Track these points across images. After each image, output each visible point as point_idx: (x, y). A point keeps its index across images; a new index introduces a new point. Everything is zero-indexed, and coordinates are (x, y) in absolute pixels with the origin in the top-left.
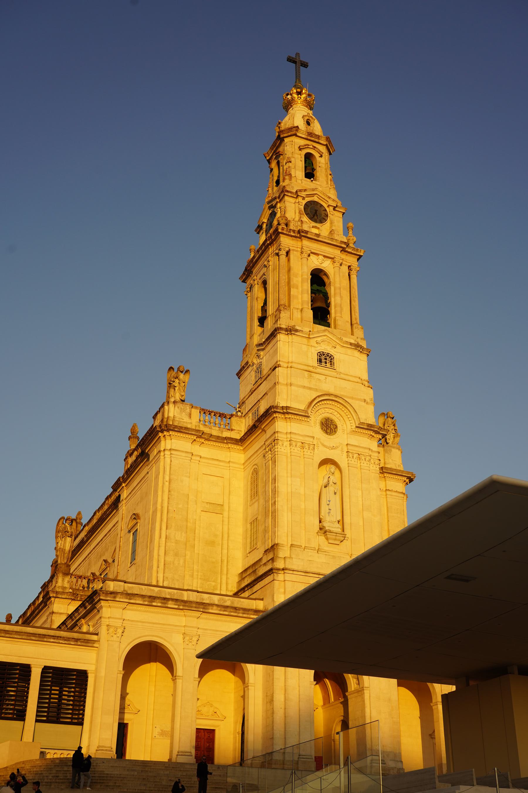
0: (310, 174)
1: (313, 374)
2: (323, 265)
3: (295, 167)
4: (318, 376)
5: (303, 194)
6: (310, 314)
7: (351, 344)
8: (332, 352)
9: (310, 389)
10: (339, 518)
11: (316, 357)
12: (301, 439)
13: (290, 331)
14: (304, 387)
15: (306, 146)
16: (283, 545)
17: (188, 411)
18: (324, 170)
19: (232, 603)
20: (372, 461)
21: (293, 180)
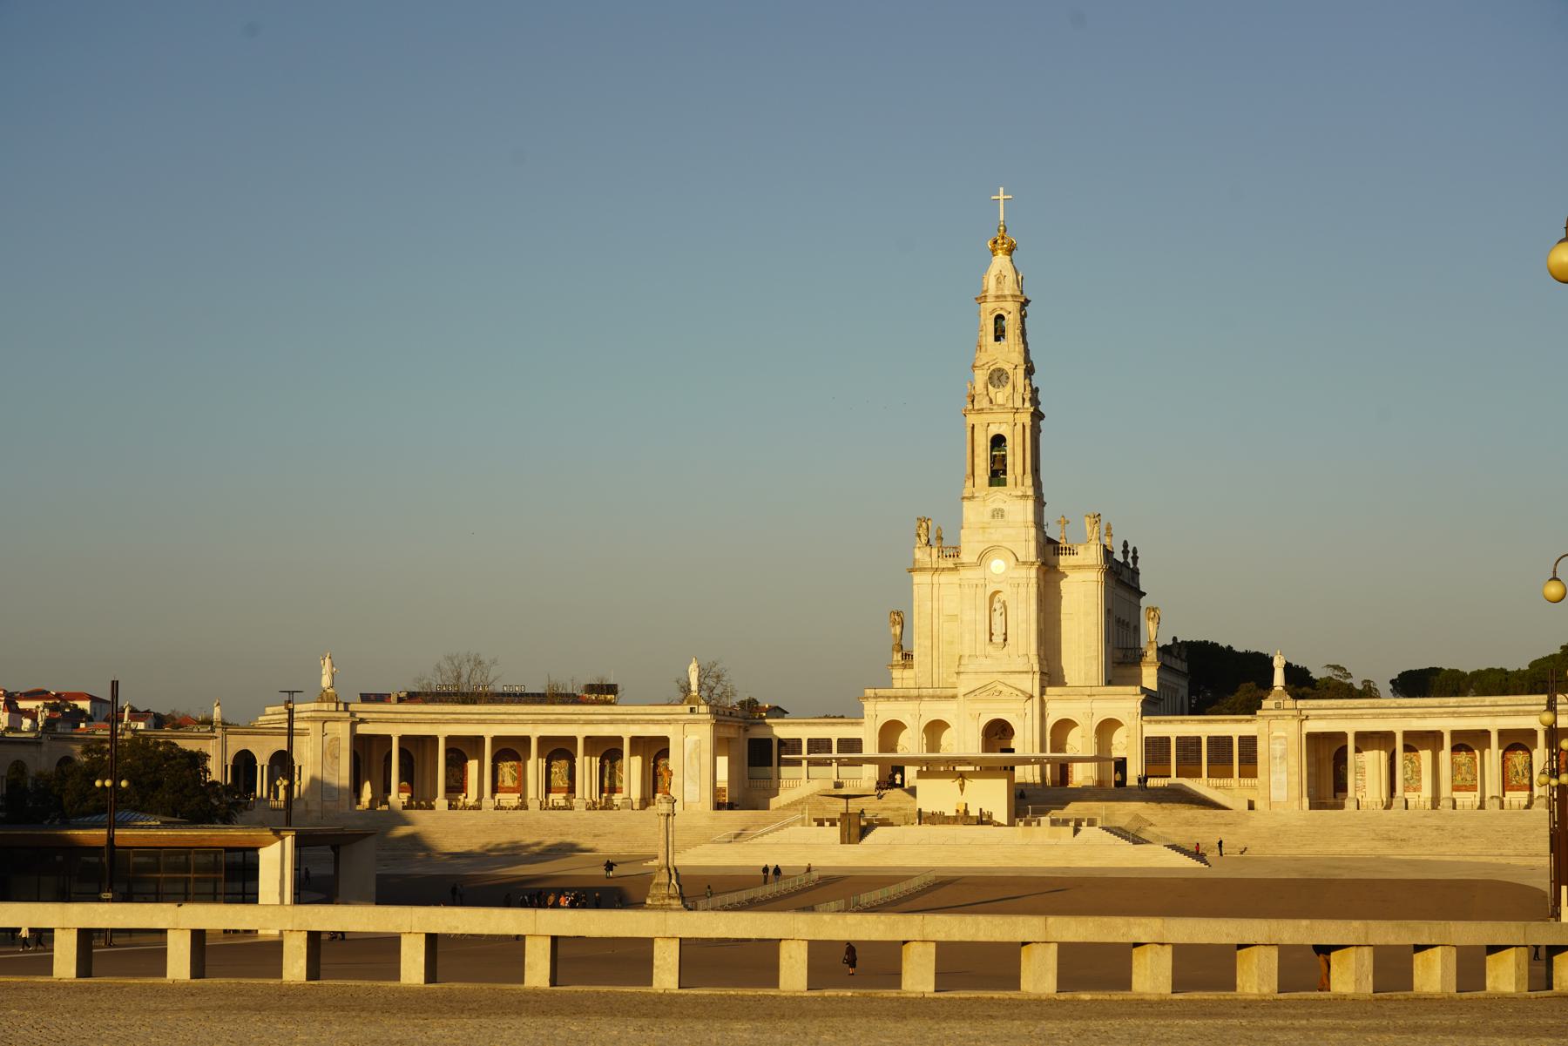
0: (999, 335)
1: (987, 530)
2: (1001, 430)
3: (986, 336)
4: (990, 530)
5: (986, 367)
6: (986, 479)
7: (1017, 496)
8: (1002, 506)
9: (983, 542)
10: (1004, 631)
11: (990, 514)
12: (976, 582)
13: (972, 498)
14: (978, 542)
15: (995, 310)
16: (964, 656)
17: (929, 552)
18: (1012, 326)
19: (941, 692)
20: (1030, 585)
21: (983, 349)
